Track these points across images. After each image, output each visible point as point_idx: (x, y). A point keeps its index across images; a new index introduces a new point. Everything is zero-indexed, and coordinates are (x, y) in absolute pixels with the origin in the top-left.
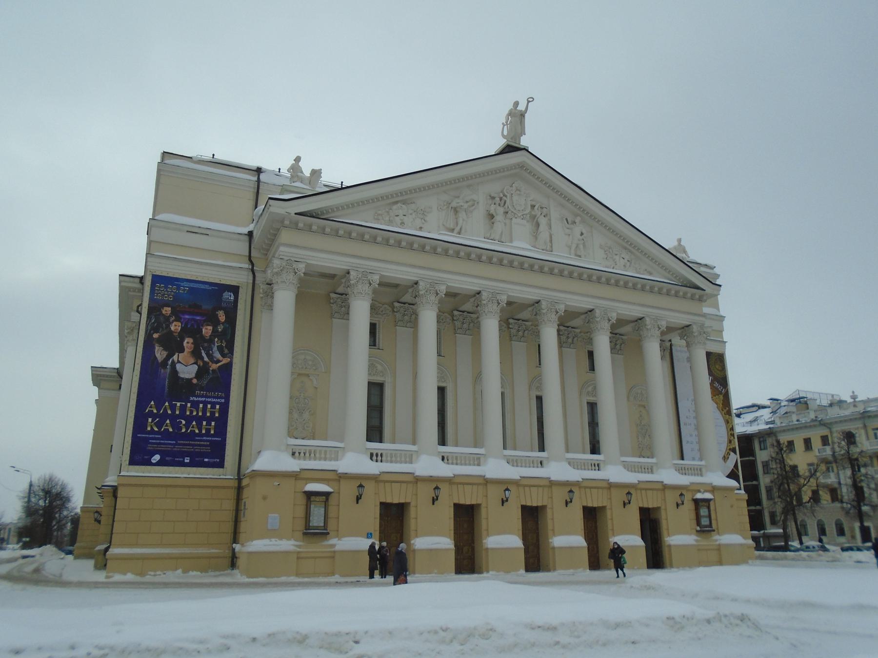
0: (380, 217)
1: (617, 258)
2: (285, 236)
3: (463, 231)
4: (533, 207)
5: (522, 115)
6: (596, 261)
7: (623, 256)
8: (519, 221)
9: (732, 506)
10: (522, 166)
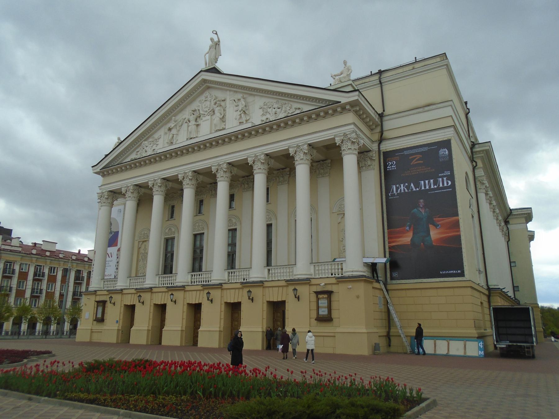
0: (139, 153)
6: (257, 118)
9: (358, 297)
10: (204, 81)
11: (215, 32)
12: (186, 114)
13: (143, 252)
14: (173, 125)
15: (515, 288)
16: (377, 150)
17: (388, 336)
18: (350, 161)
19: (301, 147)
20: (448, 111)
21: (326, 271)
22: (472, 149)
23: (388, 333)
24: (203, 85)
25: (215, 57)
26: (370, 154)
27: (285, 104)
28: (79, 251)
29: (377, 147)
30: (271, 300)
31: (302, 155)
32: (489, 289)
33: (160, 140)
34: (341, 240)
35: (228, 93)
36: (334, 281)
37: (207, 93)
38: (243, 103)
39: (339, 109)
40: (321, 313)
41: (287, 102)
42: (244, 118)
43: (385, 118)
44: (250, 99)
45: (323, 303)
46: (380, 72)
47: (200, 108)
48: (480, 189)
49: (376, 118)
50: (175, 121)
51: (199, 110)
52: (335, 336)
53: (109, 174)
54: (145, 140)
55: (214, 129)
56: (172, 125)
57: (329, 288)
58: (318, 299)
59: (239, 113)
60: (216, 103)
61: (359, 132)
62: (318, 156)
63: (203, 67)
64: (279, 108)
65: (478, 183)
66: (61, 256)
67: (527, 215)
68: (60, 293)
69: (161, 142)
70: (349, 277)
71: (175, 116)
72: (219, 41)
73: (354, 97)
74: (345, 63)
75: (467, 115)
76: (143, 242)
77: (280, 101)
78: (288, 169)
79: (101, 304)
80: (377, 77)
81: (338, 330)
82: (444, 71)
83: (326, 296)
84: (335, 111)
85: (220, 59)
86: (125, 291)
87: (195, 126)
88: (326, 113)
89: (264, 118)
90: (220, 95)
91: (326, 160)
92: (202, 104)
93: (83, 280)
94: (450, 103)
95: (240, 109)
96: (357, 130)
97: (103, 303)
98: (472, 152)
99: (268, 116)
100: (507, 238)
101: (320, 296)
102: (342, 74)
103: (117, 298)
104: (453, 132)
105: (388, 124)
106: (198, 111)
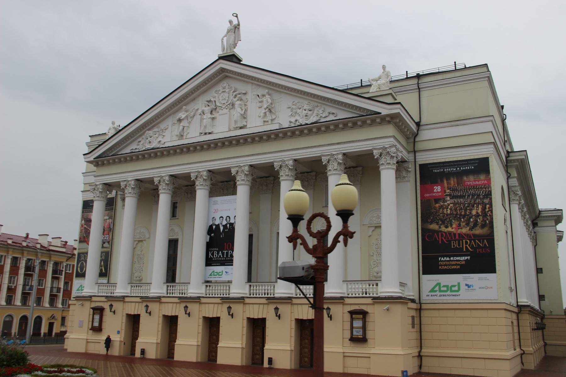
3: (185, 134)
5: (237, 28)
6: (284, 119)
7: (304, 108)
8: (225, 111)
10: (222, 70)
11: (235, 15)
12: (200, 105)
13: (139, 253)
14: (183, 116)
15: (541, 298)
16: (413, 160)
17: (420, 357)
18: (388, 176)
19: (336, 157)
20: (489, 127)
21: (357, 289)
22: (506, 158)
23: (420, 352)
24: (220, 74)
25: (234, 42)
26: (405, 165)
27: (317, 106)
28: (28, 235)
29: (413, 158)
30: (300, 318)
31: (336, 165)
32: (518, 306)
33: (167, 131)
34: (372, 254)
35: (250, 85)
36: (369, 301)
37: (224, 84)
38: (269, 100)
39: (378, 120)
40: (355, 333)
41: (319, 105)
42: (269, 118)
43: (421, 128)
44: (276, 96)
45: (358, 324)
46: (418, 76)
47: (217, 100)
48: (514, 200)
49: (414, 127)
50: (186, 111)
51: (215, 101)
52: (370, 357)
53: (103, 164)
54: (149, 130)
55: (233, 125)
56: (182, 115)
57: (364, 308)
58: (352, 319)
59: (264, 111)
60: (236, 96)
61: (398, 146)
62: (350, 163)
63: (220, 53)
64: (310, 111)
65: (511, 193)
66: (10, 242)
67: (557, 217)
68: (8, 286)
69: (167, 134)
70: (385, 298)
71: (185, 105)
72: (239, 25)
73: (396, 109)
74: (384, 67)
75: (503, 121)
76: (139, 241)
77: (311, 102)
78: (314, 173)
79: (99, 312)
80: (415, 81)
81: (373, 351)
82: (486, 84)
83: (361, 316)
84: (373, 122)
85: (239, 44)
86: (127, 299)
87: (210, 120)
88: (364, 122)
89: (293, 120)
90: (241, 87)
91: (357, 167)
92: (221, 94)
93: (34, 271)
94: (491, 118)
95: (265, 106)
96: (396, 143)
97: (99, 311)
98: (506, 160)
99: (297, 117)
100: (535, 241)
101: (354, 316)
102: (380, 78)
103: (117, 306)
104: (492, 149)
105: (425, 135)
106: (214, 103)
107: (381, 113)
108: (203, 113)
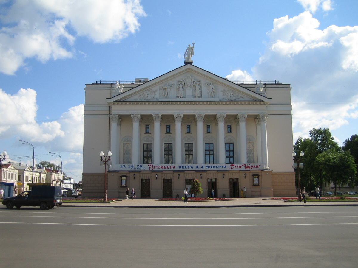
1: (228, 94)
2: (113, 107)
4: (194, 82)
10: (189, 69)
45: (256, 179)
89: (224, 97)
101: (255, 177)
107: (264, 101)
108: (179, 87)
